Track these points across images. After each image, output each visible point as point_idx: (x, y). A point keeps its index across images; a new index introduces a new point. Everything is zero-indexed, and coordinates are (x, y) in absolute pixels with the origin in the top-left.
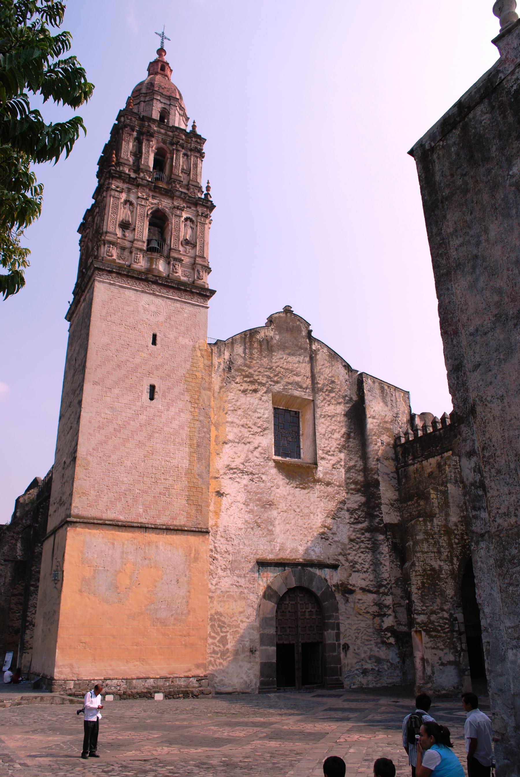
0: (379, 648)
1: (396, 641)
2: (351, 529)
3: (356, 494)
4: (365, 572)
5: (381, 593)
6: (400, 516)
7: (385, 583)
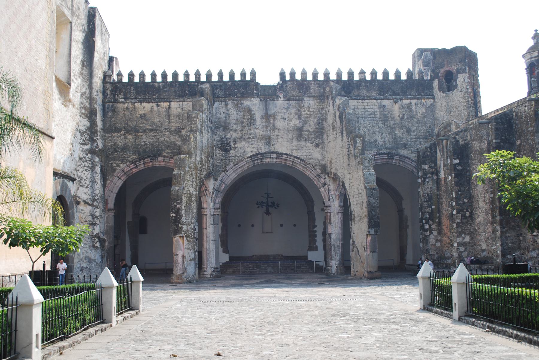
0: (91, 250)
1: (100, 245)
2: (81, 149)
3: (85, 118)
4: (86, 187)
5: (94, 206)
6: (103, 143)
7: (96, 198)
